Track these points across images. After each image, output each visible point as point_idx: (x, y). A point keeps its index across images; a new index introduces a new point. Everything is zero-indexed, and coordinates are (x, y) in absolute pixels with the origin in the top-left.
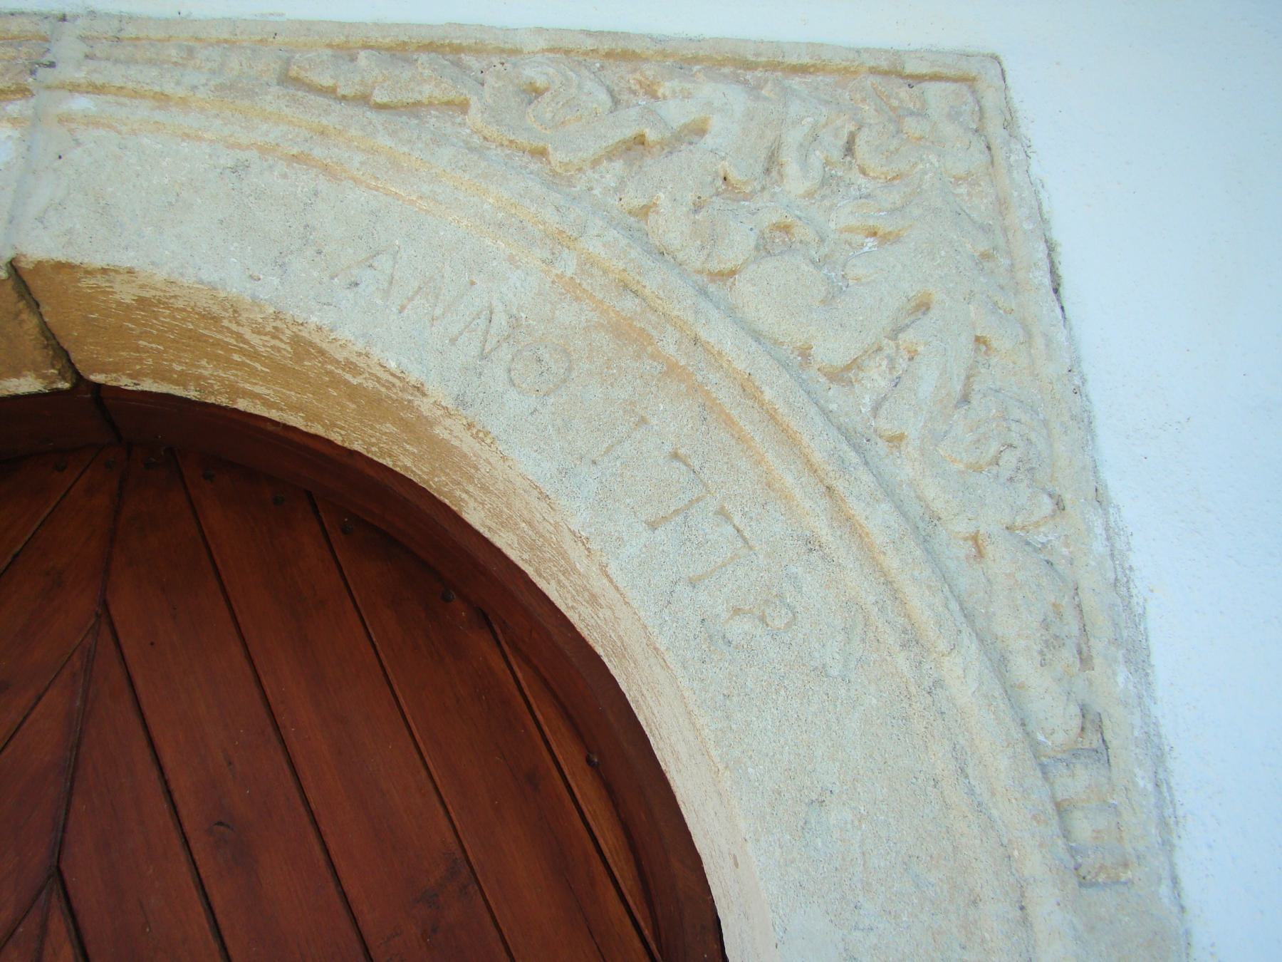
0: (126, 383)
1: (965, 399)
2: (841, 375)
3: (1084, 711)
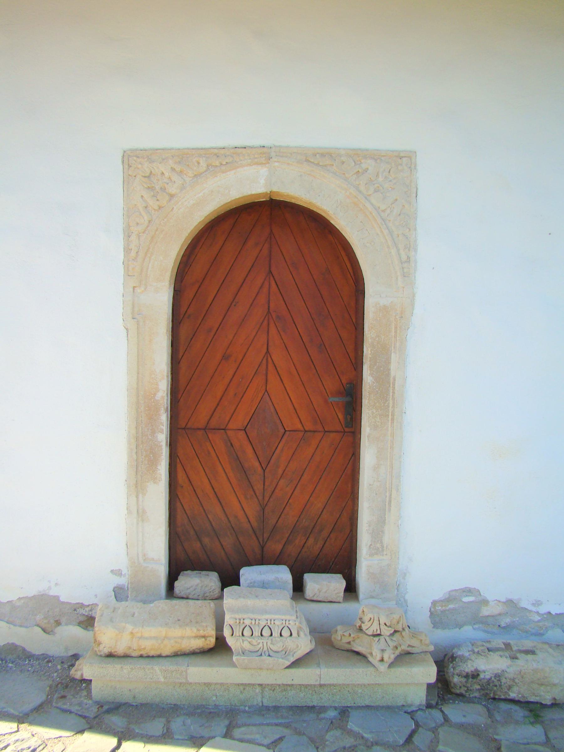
0: (278, 199)
1: (400, 215)
2: (383, 211)
3: (408, 257)
